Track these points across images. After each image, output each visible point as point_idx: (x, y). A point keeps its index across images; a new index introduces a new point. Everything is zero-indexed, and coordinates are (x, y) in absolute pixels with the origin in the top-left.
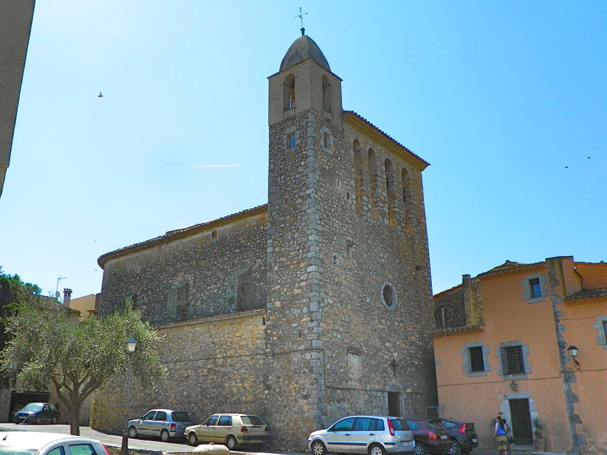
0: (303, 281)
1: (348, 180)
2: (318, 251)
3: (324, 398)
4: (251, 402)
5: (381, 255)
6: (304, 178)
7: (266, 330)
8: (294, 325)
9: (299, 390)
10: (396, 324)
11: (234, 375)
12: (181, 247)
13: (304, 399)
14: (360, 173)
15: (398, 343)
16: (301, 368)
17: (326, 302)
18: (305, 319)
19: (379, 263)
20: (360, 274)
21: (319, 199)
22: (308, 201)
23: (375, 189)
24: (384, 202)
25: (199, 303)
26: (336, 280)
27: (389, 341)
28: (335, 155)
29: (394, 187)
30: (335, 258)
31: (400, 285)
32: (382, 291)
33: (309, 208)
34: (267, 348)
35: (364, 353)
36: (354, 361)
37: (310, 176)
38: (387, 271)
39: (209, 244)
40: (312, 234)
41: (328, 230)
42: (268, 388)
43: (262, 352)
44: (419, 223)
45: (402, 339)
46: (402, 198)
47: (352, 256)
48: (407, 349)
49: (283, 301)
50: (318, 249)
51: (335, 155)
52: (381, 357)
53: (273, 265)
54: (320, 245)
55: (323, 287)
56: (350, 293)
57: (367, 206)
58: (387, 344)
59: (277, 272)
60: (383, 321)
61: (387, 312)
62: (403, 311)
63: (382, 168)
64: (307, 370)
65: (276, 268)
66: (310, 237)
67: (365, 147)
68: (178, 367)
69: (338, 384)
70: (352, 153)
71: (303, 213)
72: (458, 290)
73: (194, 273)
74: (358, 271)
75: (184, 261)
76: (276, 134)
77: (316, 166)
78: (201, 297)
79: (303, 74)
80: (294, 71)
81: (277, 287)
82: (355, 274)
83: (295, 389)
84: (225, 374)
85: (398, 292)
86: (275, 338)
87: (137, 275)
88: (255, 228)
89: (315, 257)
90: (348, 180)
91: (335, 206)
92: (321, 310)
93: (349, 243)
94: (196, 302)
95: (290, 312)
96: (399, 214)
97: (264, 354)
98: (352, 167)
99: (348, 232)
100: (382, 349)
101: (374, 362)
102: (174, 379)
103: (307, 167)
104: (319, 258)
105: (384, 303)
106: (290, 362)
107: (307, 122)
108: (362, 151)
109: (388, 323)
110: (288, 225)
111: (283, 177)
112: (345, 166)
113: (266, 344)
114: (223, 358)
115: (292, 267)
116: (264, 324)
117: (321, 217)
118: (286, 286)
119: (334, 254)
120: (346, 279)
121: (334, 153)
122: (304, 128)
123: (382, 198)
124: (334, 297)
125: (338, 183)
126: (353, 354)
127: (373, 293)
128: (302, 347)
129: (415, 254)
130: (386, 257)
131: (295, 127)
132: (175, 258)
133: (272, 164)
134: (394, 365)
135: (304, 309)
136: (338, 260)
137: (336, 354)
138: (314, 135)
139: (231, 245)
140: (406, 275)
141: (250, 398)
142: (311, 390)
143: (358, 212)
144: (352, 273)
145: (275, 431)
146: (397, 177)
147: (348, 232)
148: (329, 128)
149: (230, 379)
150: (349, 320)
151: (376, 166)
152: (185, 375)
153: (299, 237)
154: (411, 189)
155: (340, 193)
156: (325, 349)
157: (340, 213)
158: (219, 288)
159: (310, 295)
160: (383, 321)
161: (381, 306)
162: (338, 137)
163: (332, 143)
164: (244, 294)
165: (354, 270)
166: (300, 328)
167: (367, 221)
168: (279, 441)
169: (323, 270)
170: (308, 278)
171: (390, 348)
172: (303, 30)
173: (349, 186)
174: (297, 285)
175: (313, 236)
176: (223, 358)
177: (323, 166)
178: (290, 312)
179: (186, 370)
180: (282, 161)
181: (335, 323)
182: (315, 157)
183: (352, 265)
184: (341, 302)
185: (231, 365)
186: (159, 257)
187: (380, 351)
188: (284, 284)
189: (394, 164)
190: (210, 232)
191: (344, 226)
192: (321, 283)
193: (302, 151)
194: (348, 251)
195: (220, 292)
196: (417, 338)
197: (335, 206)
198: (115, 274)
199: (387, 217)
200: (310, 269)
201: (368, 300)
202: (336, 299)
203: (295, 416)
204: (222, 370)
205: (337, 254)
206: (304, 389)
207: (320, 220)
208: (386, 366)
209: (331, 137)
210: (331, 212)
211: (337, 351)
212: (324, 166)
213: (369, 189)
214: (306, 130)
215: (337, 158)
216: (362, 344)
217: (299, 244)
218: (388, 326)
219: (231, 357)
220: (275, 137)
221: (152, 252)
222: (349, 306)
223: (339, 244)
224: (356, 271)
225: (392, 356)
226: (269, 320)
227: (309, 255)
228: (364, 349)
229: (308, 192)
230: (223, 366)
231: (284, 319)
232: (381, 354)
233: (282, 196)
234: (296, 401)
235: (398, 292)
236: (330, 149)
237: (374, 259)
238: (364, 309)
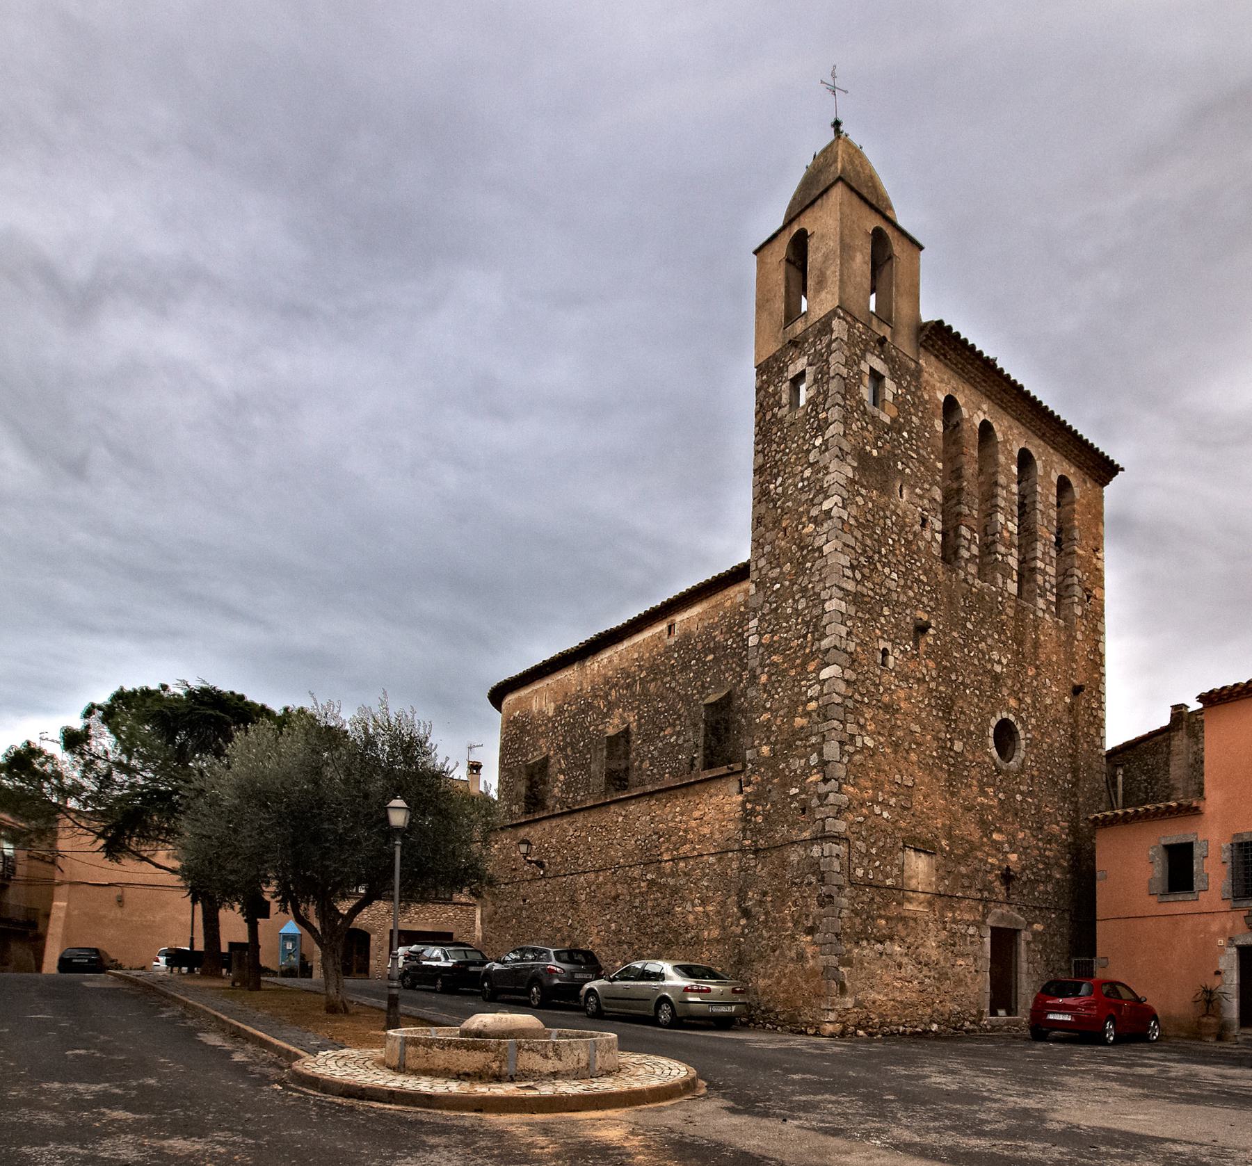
0: (811, 699)
1: (926, 486)
2: (844, 634)
3: (846, 933)
4: (718, 941)
5: (996, 657)
6: (820, 475)
7: (743, 804)
8: (794, 791)
9: (800, 916)
10: (1019, 797)
11: (691, 893)
12: (616, 660)
13: (808, 934)
14: (957, 474)
15: (1021, 835)
16: (804, 875)
17: (859, 744)
18: (812, 779)
19: (987, 672)
20: (941, 692)
21: (852, 522)
22: (825, 525)
23: (990, 515)
24: (1010, 545)
25: (646, 764)
26: (886, 699)
27: (999, 831)
28: (896, 425)
29: (1035, 515)
30: (885, 653)
31: (1033, 721)
32: (991, 731)
33: (828, 541)
34: (745, 838)
35: (942, 850)
36: (919, 867)
37: (832, 467)
38: (1005, 692)
39: (662, 650)
40: (831, 598)
41: (871, 593)
42: (746, 913)
43: (736, 847)
44: (1089, 597)
45: (1030, 828)
46: (1054, 539)
47: (926, 653)
48: (1039, 849)
49: (775, 743)
50: (843, 631)
51: (896, 425)
52: (981, 860)
53: (758, 671)
54: (849, 623)
55: (856, 711)
56: (917, 728)
57: (968, 549)
58: (995, 836)
59: (765, 685)
60: (990, 790)
61: (999, 774)
62: (1036, 773)
63: (1010, 470)
64: (813, 879)
65: (764, 678)
66: (827, 605)
67: (971, 417)
68: (601, 878)
69: (879, 908)
70: (939, 426)
71: (817, 555)
72: (1160, 738)
73: (638, 707)
74: (938, 684)
75: (622, 687)
76: (768, 382)
77: (847, 448)
78: (650, 752)
79: (825, 224)
80: (806, 222)
81: (766, 716)
82: (930, 691)
83: (792, 916)
84: (675, 890)
85: (1029, 736)
86: (760, 819)
87: (549, 719)
88: (742, 609)
89: (835, 647)
90: (926, 486)
91: (891, 542)
92: (845, 760)
93: (920, 623)
94: (642, 762)
95: (787, 766)
96: (1044, 573)
97: (740, 850)
98: (937, 458)
99: (919, 601)
100: (983, 844)
101: (963, 870)
102: (596, 900)
103: (827, 449)
104: (845, 651)
105: (995, 753)
106: (784, 863)
107: (831, 342)
108: (966, 426)
109: (1001, 795)
110: (787, 583)
111: (780, 480)
112: (918, 454)
113: (744, 830)
114: (673, 860)
115: (793, 673)
116: (741, 792)
117: (855, 563)
118: (781, 713)
119: (883, 645)
120: (908, 699)
121: (894, 420)
122: (820, 360)
123: (1006, 534)
124: (879, 734)
125: (901, 491)
126: (916, 850)
127: (971, 733)
128: (806, 835)
129: (1075, 661)
130: (1005, 661)
131: (804, 360)
132: (607, 682)
133: (761, 455)
134: (1007, 877)
135: (812, 758)
136: (891, 658)
137: (878, 848)
138: (844, 372)
139: (699, 646)
140: (1048, 701)
141: (715, 933)
142: (820, 916)
143: (945, 559)
144: (923, 688)
145: (756, 993)
146: (1046, 495)
147: (919, 601)
148: (885, 361)
149: (683, 899)
150: (910, 784)
151: (997, 464)
152: (613, 894)
153: (807, 607)
154: (1076, 523)
155: (905, 513)
156: (852, 838)
157: (900, 558)
158: (679, 734)
159: (824, 727)
160: (990, 790)
161: (987, 759)
162: (905, 384)
163: (889, 397)
164: (719, 740)
165: (928, 683)
166: (803, 796)
167: (965, 580)
168: (763, 1012)
169: (854, 677)
170: (821, 694)
171: (1002, 843)
172: (837, 124)
173: (926, 501)
174: (800, 709)
175: (834, 601)
176: (673, 860)
177: (863, 449)
178: (787, 766)
179: (615, 884)
180: (779, 445)
181: (877, 786)
182: (845, 423)
183: (925, 672)
184: (896, 746)
185: (685, 874)
186: (581, 684)
187: (979, 849)
188: (777, 710)
189: (1039, 463)
190: (662, 627)
191: (911, 588)
192: (850, 703)
193: (818, 413)
194: (916, 643)
195: (680, 742)
196: (1062, 828)
197: (891, 542)
198: (516, 721)
199: (1015, 578)
200: (825, 673)
201: (958, 746)
202: (882, 740)
203: (791, 966)
204: (671, 881)
205: (889, 646)
206: (807, 916)
207: (852, 567)
208: (991, 877)
209: (888, 382)
210: (880, 552)
211: (881, 844)
212: (868, 448)
213: (975, 512)
214: (827, 361)
215: (899, 432)
216: (940, 833)
217: (807, 624)
218: (1001, 802)
219: (685, 858)
220: (767, 392)
221: (570, 676)
222: (913, 757)
223: (896, 626)
224: (933, 685)
225: (1006, 859)
226: (749, 783)
227: (825, 643)
228: (944, 842)
229: (826, 505)
230: (673, 874)
231: (776, 781)
232: (979, 854)
233: (777, 522)
234: (793, 937)
235: (1029, 736)
236: (883, 410)
237: (976, 662)
238: (948, 764)
